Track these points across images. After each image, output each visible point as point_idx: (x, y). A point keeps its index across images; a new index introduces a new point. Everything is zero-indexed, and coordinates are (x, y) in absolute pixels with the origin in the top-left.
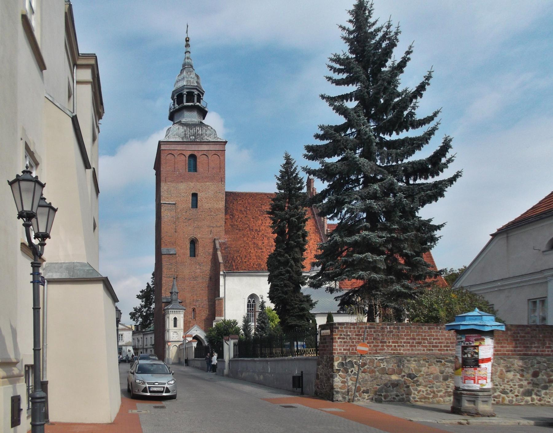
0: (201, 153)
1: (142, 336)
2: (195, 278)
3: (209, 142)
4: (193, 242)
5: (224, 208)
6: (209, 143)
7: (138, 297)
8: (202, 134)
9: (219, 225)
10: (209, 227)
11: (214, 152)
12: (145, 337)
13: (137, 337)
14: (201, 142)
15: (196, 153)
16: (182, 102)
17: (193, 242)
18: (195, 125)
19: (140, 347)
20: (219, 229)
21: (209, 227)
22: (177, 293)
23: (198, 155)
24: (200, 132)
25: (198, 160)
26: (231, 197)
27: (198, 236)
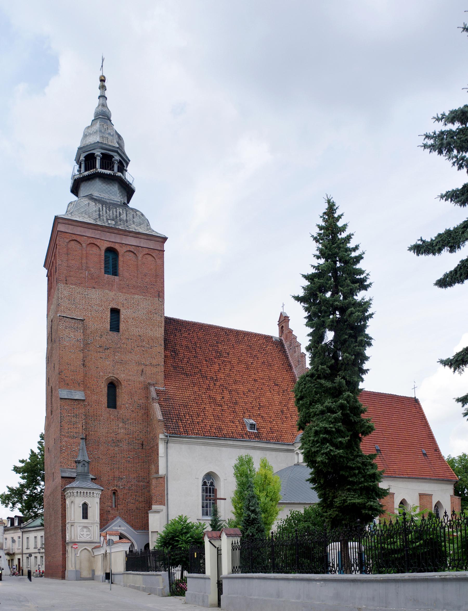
0: (125, 249)
1: (20, 534)
2: (117, 442)
3: (139, 233)
4: (113, 386)
5: (163, 337)
6: (137, 235)
7: (17, 470)
8: (127, 221)
9: (154, 362)
10: (139, 364)
11: (146, 251)
12: (25, 536)
13: (12, 535)
14: (125, 231)
15: (117, 247)
16: (94, 167)
17: (113, 386)
18: (115, 205)
19: (16, 551)
20: (155, 370)
21: (139, 364)
22: (88, 463)
23: (121, 250)
24: (124, 217)
25: (121, 259)
26: (169, 322)
27: (122, 377)
